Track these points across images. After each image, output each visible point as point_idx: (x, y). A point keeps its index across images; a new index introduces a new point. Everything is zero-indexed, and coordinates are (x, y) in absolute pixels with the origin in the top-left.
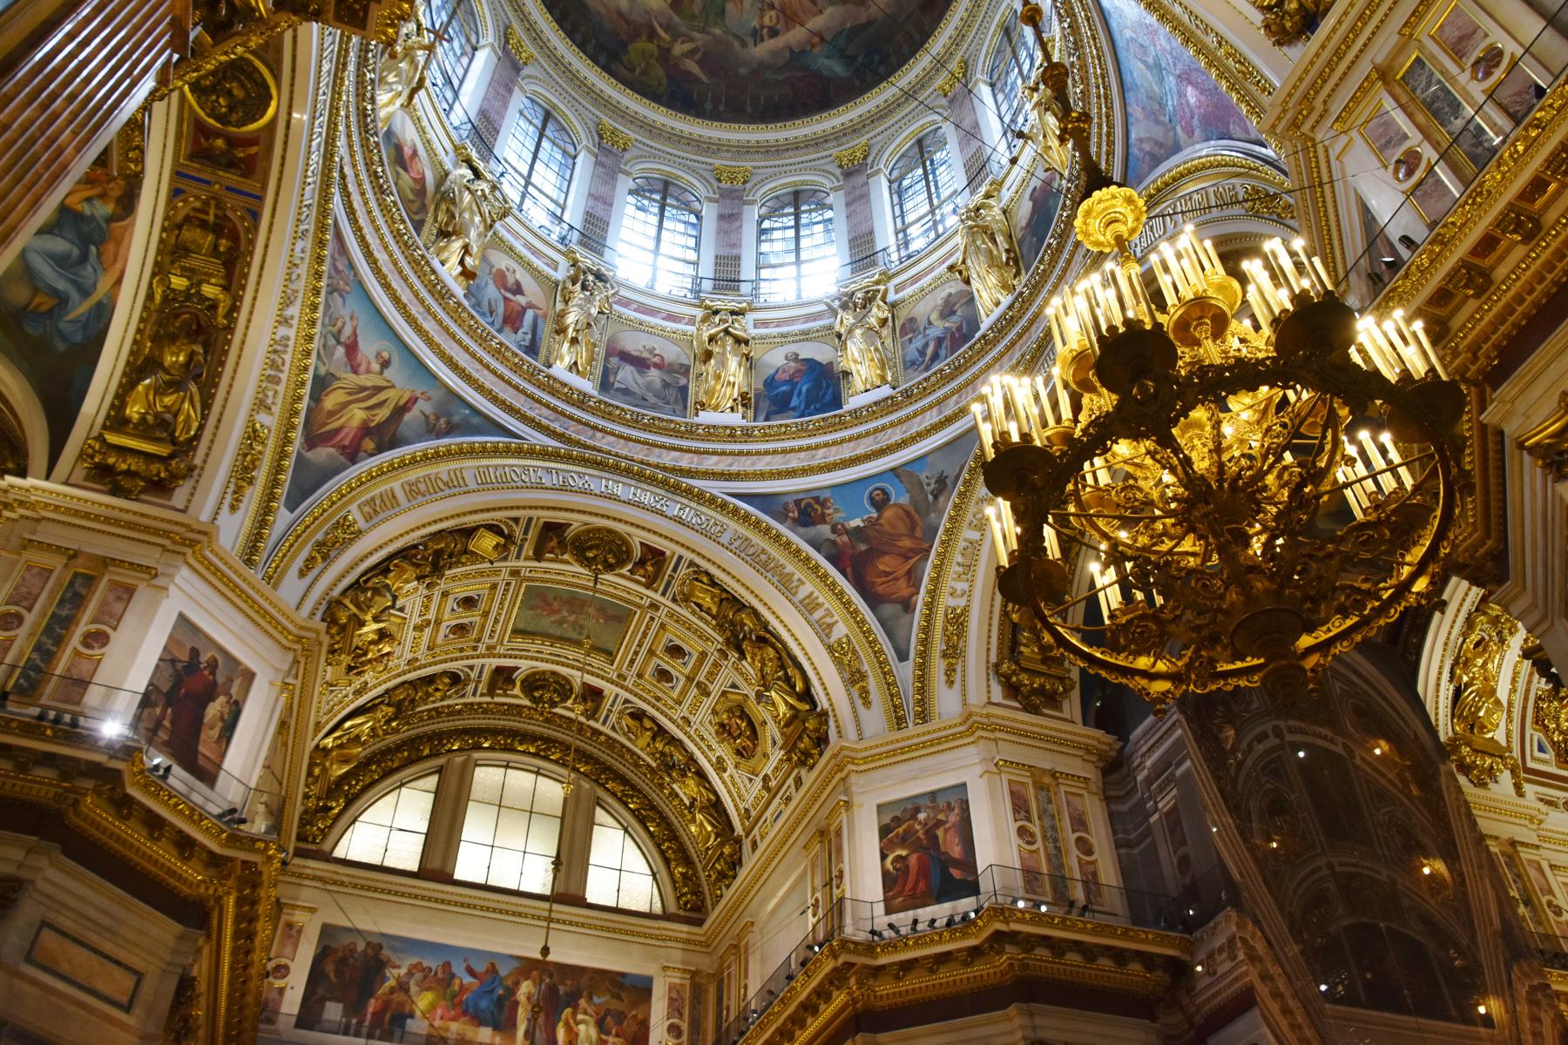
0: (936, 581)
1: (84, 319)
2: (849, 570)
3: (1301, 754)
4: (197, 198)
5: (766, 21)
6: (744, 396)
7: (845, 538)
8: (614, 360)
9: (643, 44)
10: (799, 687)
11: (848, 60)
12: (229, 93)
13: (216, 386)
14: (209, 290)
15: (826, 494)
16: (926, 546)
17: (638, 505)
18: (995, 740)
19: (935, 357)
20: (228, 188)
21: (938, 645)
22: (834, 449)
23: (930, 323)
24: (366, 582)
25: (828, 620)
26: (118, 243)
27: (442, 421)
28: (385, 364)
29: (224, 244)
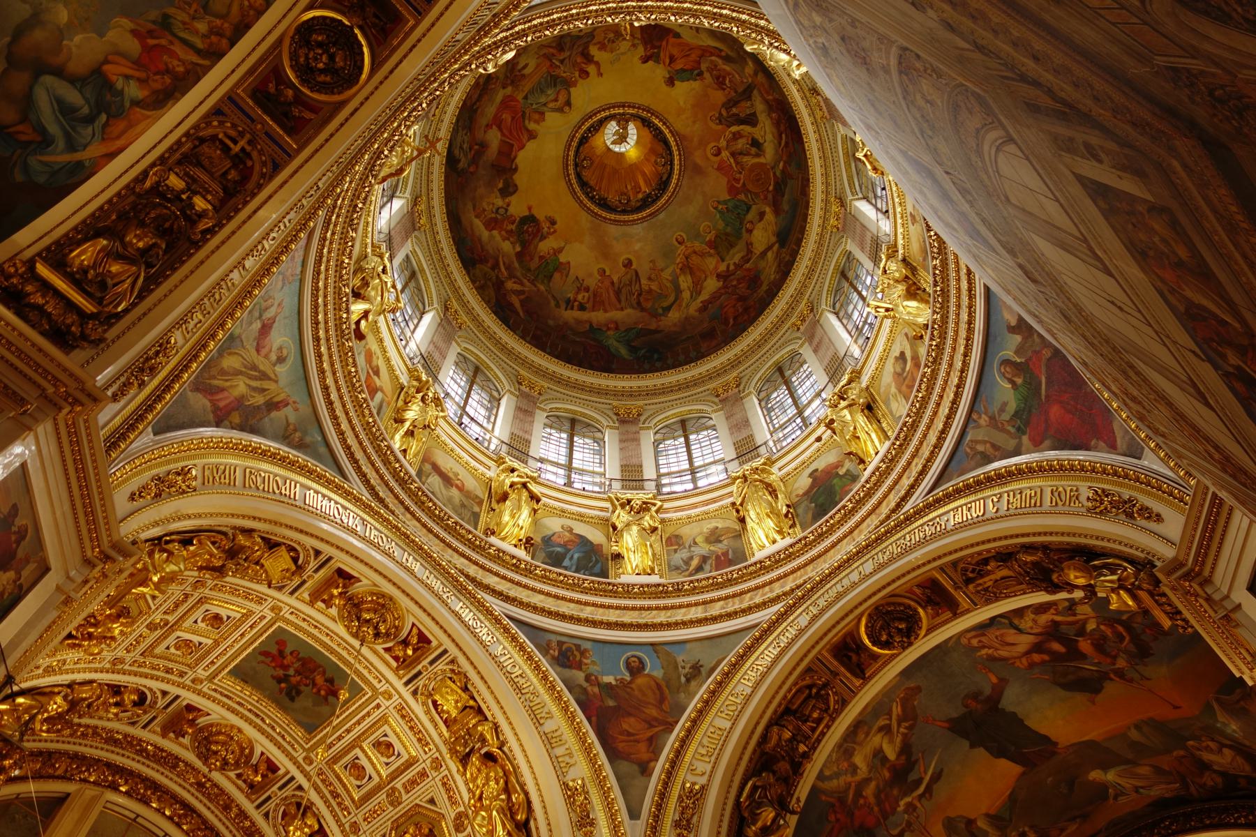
0: (679, 752)
1: (56, 167)
2: (594, 719)
4: (234, 126)
5: (580, 297)
6: (529, 540)
7: (596, 690)
8: (428, 467)
9: (486, 268)
11: (633, 349)
12: (332, 57)
13: (158, 285)
14: (200, 203)
15: (588, 645)
16: (670, 720)
17: (429, 588)
19: (699, 569)
20: (266, 134)
22: (601, 610)
23: (695, 543)
24: (167, 542)
25: (567, 759)
26: (131, 126)
27: (298, 434)
28: (281, 360)
29: (233, 175)
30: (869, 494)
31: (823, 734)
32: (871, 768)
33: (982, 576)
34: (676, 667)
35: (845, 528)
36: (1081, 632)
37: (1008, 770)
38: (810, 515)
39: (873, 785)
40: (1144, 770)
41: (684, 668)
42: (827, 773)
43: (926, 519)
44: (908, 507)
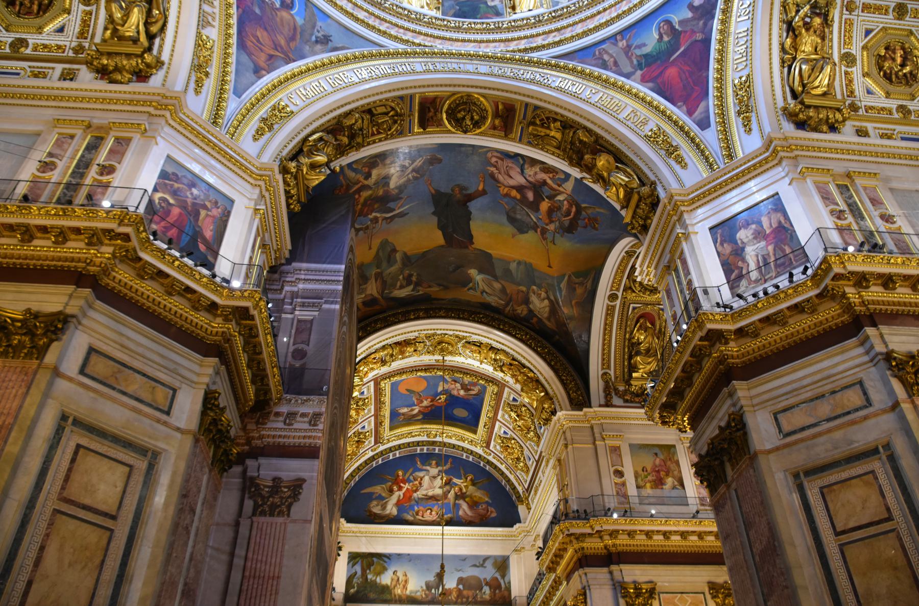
3: (285, 339)
10: (154, 29)
16: (291, 56)
18: (263, 196)
21: (263, 111)
25: (210, 19)
30: (509, 29)
31: (374, 142)
32: (376, 183)
33: (542, 126)
34: (314, 27)
35: (479, 37)
36: (551, 198)
37: (438, 239)
38: (452, 12)
39: (370, 192)
40: (497, 286)
41: (318, 31)
42: (354, 166)
43: (540, 70)
44: (535, 55)
